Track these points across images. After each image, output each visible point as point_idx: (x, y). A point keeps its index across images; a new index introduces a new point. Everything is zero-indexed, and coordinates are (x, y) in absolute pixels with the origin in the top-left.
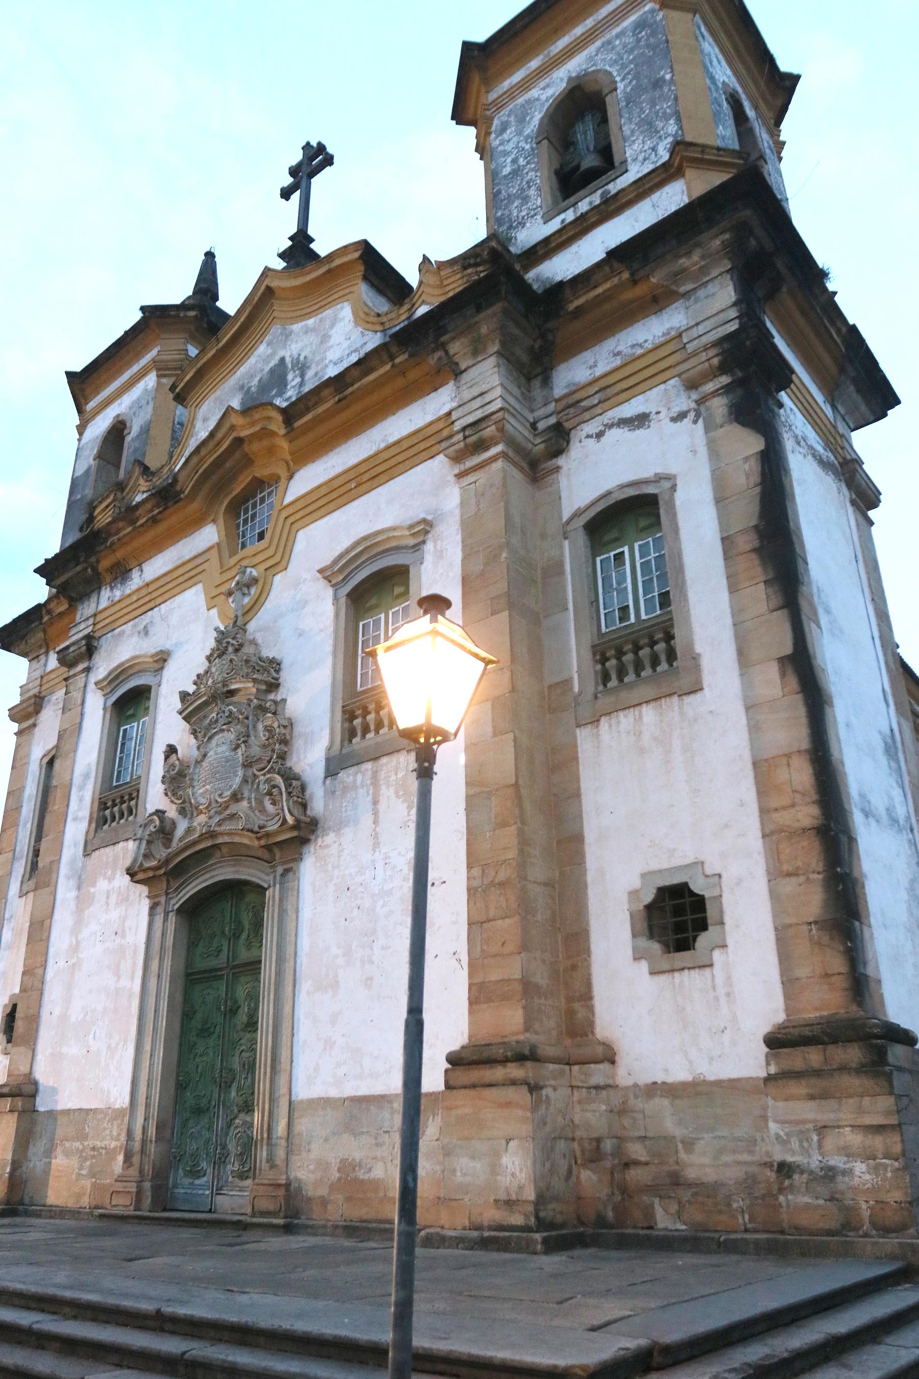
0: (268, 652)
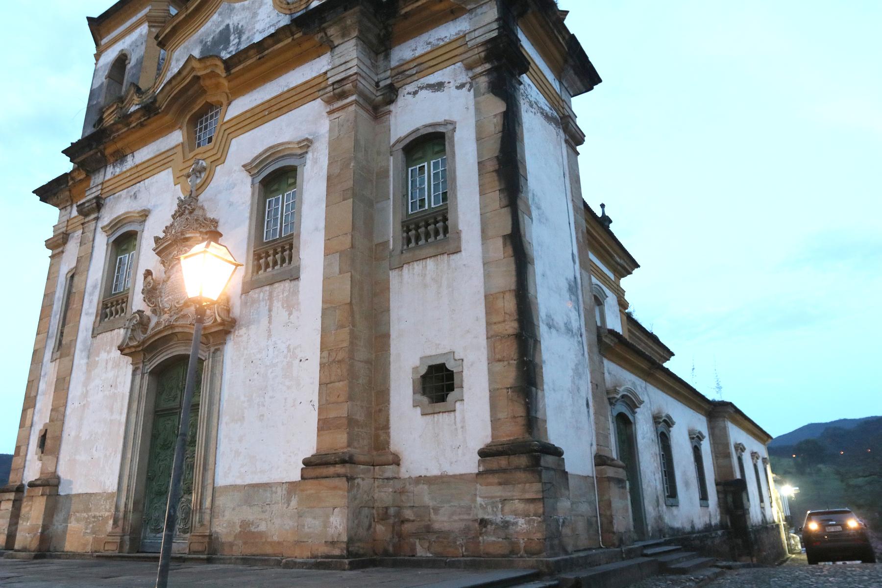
0: (210, 215)
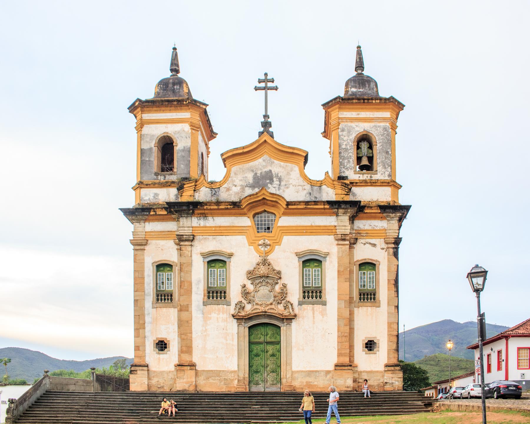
0: (277, 268)
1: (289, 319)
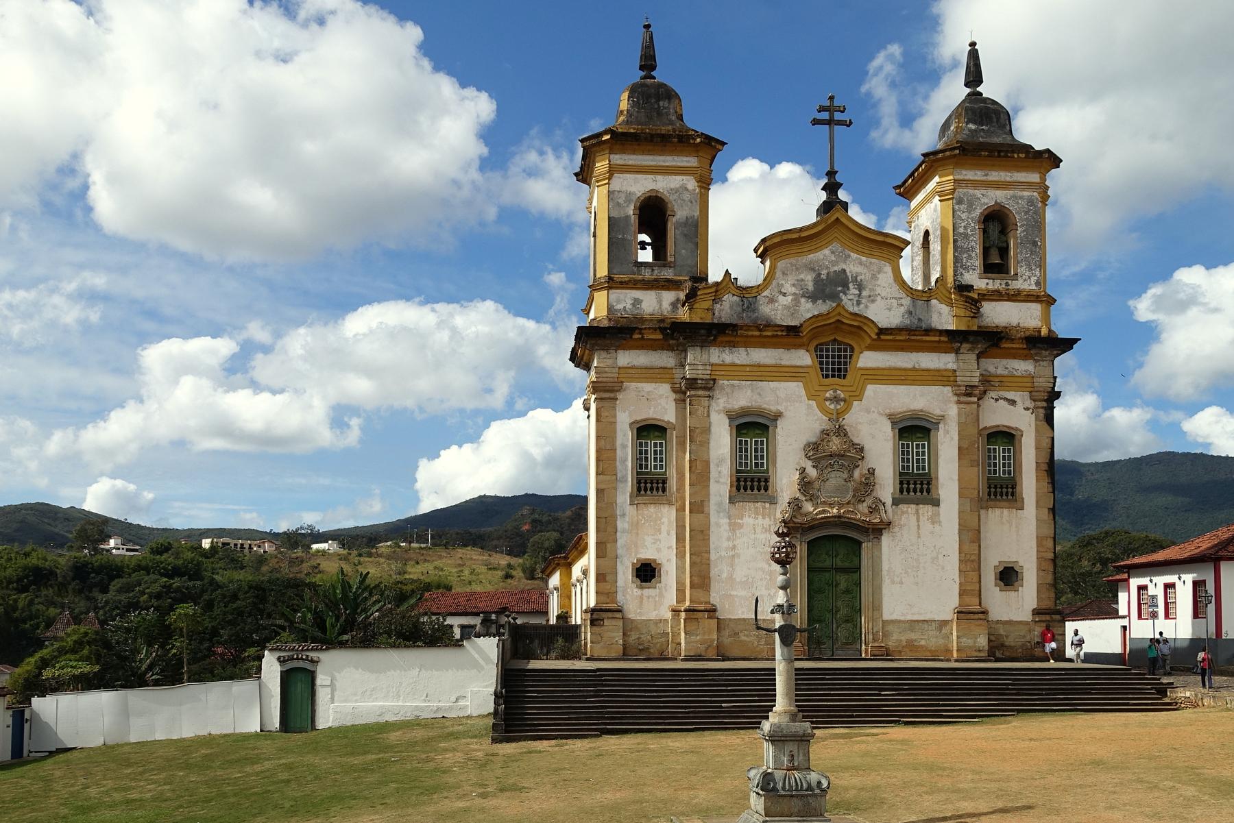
0: (856, 441)
1: (877, 531)
